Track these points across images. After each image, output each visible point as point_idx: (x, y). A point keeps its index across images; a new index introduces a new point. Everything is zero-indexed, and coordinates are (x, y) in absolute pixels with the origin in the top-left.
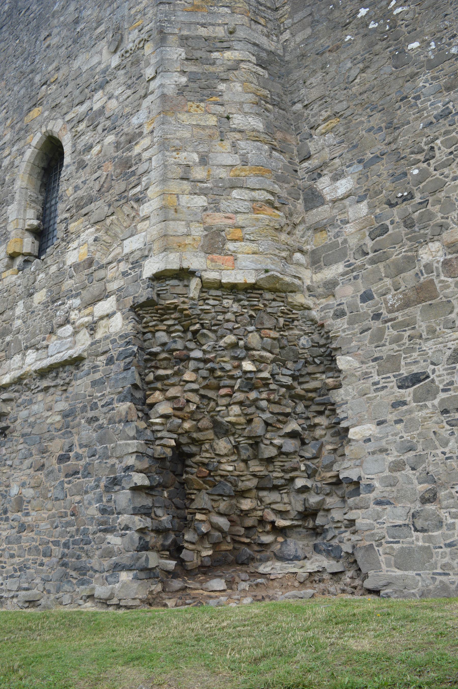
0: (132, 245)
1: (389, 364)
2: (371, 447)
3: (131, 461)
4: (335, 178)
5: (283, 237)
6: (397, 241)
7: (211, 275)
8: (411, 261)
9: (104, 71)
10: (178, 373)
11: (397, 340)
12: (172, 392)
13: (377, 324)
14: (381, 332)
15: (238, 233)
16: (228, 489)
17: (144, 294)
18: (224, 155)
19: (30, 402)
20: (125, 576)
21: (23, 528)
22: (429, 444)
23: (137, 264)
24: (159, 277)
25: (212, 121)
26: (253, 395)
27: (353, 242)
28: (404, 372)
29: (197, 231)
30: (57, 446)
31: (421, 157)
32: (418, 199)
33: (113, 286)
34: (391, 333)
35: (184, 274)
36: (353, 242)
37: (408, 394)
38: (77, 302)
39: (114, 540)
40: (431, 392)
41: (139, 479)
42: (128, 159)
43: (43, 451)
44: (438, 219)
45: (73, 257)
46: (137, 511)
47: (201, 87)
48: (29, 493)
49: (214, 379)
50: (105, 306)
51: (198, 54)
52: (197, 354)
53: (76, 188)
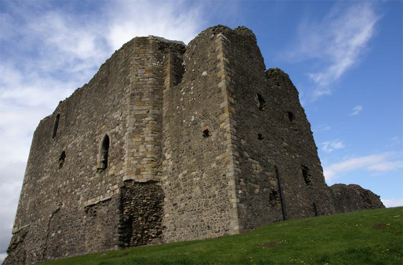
0: (121, 172)
1: (172, 200)
3: (118, 222)
4: (168, 154)
5: (155, 169)
7: (137, 180)
8: (177, 177)
9: (119, 120)
10: (130, 203)
12: (128, 207)
13: (171, 191)
14: (171, 193)
15: (144, 169)
16: (141, 228)
17: (123, 185)
18: (142, 149)
19: (101, 208)
20: (116, 246)
21: (99, 238)
22: (176, 219)
23: (122, 178)
24: (126, 181)
25: (140, 139)
26: (145, 207)
28: (174, 203)
29: (135, 170)
30: (106, 219)
31: (181, 152)
33: (118, 182)
35: (131, 181)
38: (111, 184)
39: (115, 239)
41: (119, 226)
42: (122, 149)
43: (103, 220)
45: (111, 172)
46: (119, 233)
47: (138, 131)
48: (100, 230)
49: (137, 204)
50: (116, 186)
51: (139, 120)
52: (134, 198)
53: (112, 154)
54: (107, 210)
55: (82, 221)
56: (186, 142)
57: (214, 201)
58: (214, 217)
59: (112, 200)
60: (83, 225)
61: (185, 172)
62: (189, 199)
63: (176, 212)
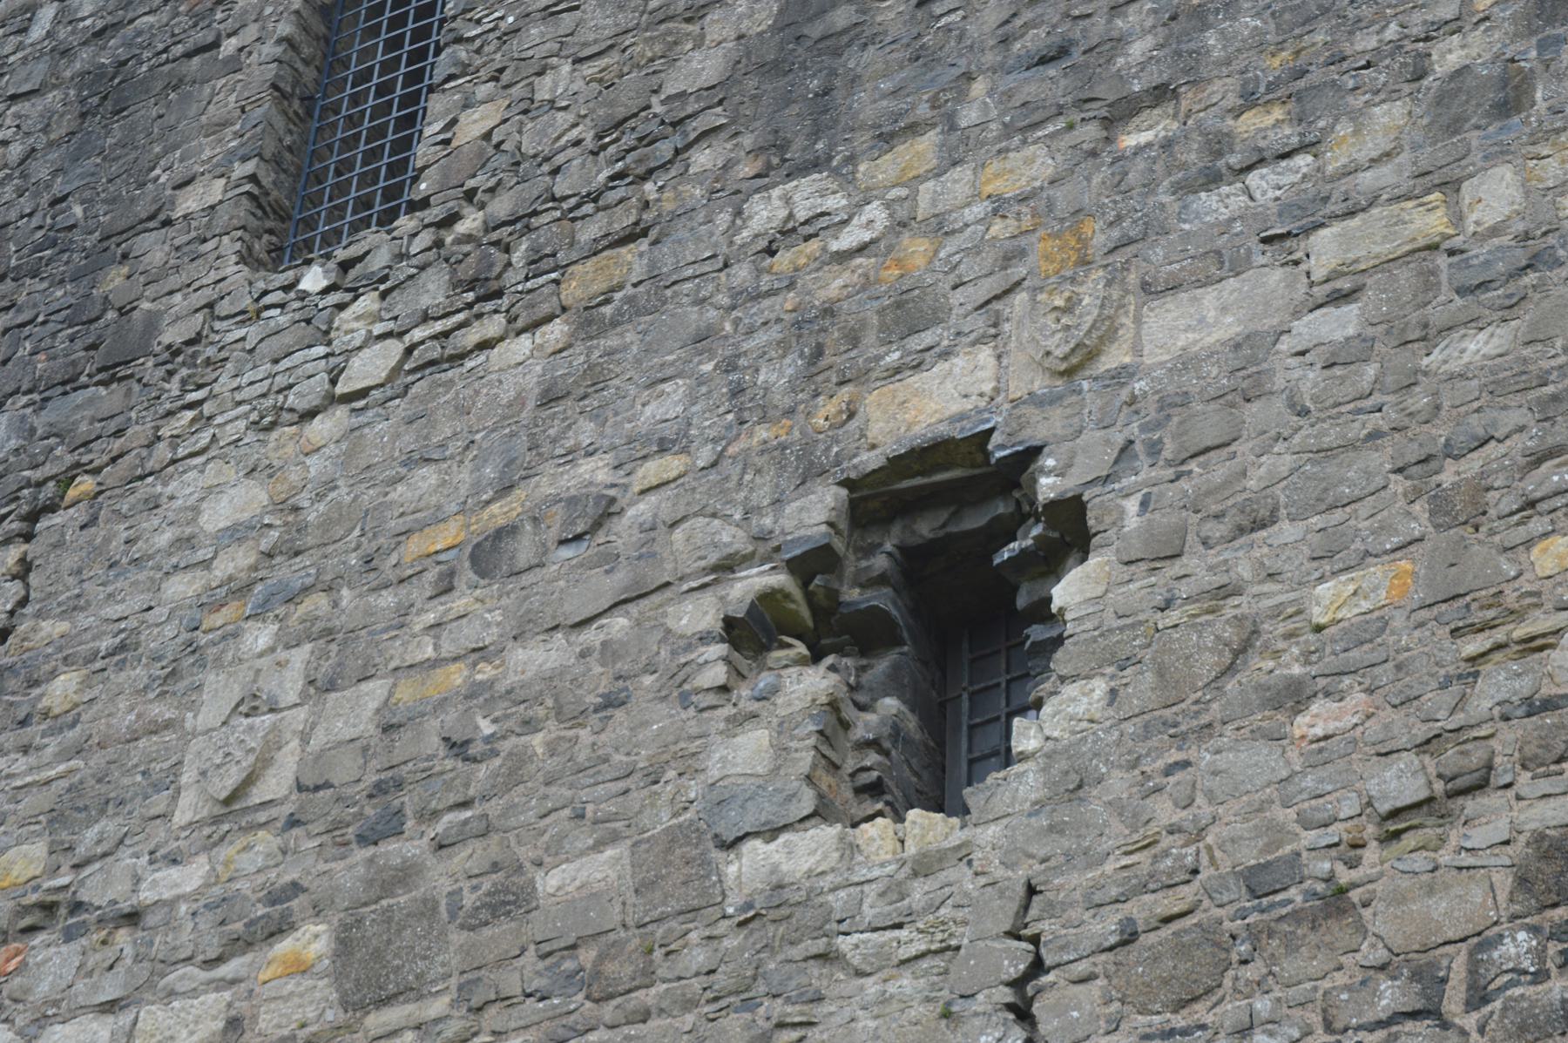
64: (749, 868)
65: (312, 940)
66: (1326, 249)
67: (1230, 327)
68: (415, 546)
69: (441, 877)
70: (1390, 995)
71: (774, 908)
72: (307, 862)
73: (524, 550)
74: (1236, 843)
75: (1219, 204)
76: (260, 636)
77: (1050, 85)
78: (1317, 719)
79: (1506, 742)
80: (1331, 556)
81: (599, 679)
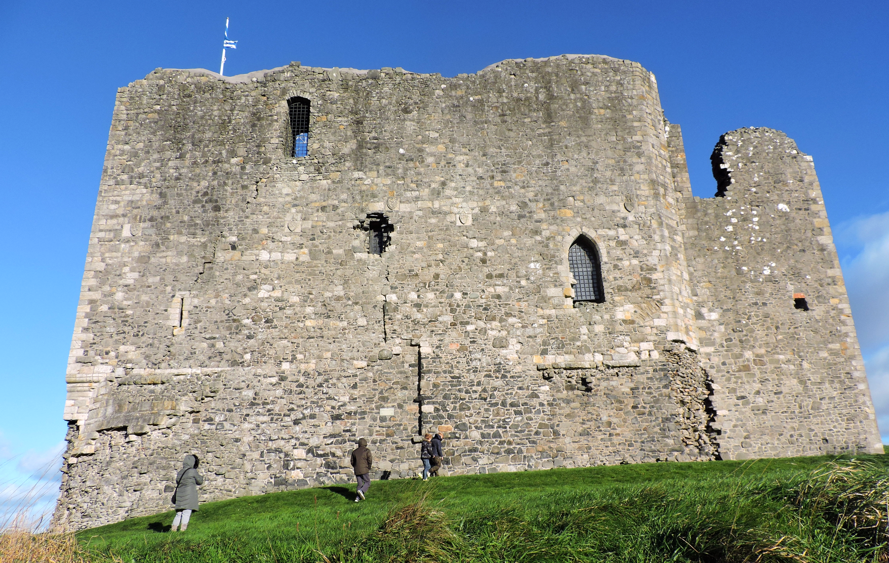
2: (726, 418)
6: (736, 346)
8: (741, 356)
11: (736, 382)
27: (718, 341)
28: (739, 394)
32: (744, 333)
34: (733, 380)
36: (718, 341)
37: (740, 402)
38: (628, 338)
40: (748, 403)
44: (752, 343)
48: (614, 420)
54: (632, 385)
55: (535, 395)
56: (756, 304)
57: (832, 406)
58: (835, 427)
59: (641, 369)
60: (542, 404)
61: (762, 351)
62: (776, 393)
63: (747, 410)
64: (358, 255)
65: (306, 250)
66: (420, 204)
67: (409, 210)
68: (313, 204)
69: (320, 247)
70: (422, 285)
71: (359, 260)
72: (304, 241)
73: (328, 209)
74: (408, 266)
75: (408, 194)
76: (293, 210)
77: (389, 171)
78: (416, 256)
79: (433, 262)
80: (418, 239)
81: (339, 230)
